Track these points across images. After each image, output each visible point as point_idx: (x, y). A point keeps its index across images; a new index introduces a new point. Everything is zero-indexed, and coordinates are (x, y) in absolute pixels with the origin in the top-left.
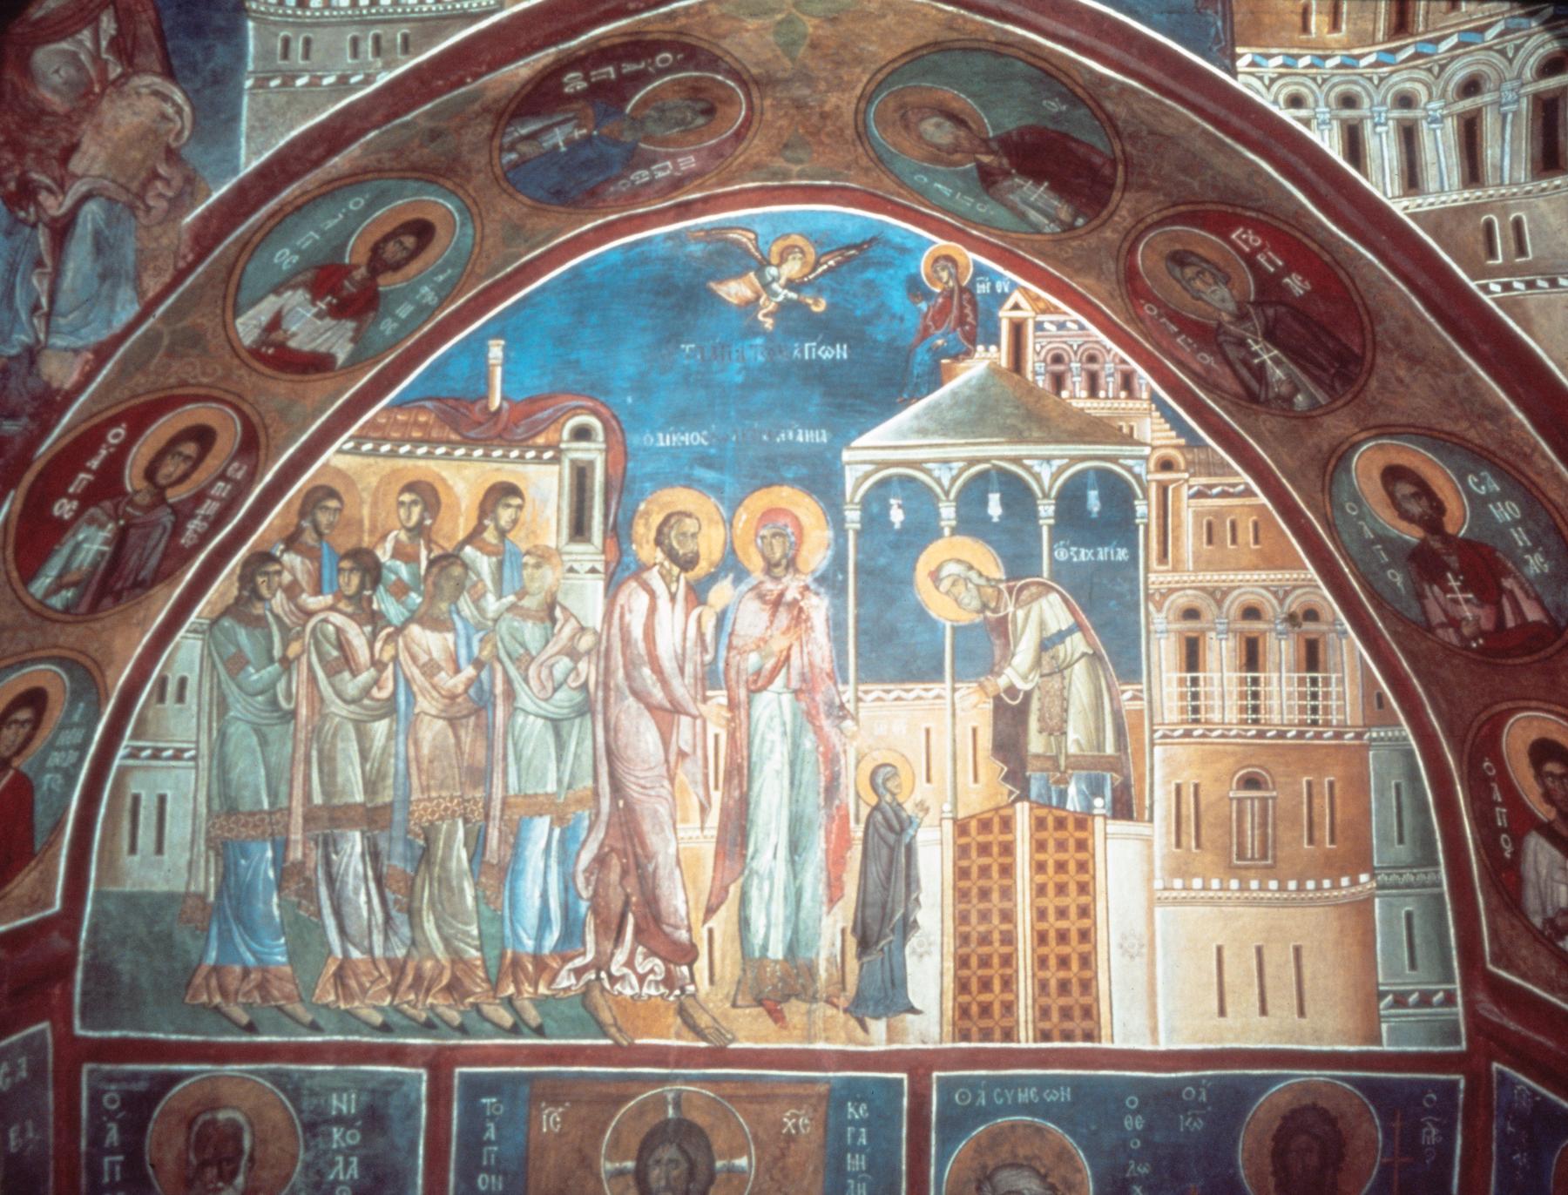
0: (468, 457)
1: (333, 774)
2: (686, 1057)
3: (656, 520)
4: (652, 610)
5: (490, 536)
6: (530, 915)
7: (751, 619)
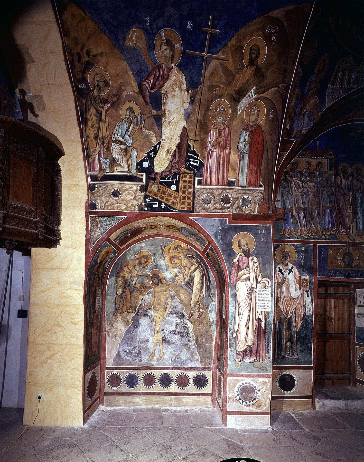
0: (314, 158)
1: (298, 203)
2: (349, 243)
3: (341, 167)
4: (341, 180)
5: (318, 169)
6: (327, 223)
7: (355, 182)
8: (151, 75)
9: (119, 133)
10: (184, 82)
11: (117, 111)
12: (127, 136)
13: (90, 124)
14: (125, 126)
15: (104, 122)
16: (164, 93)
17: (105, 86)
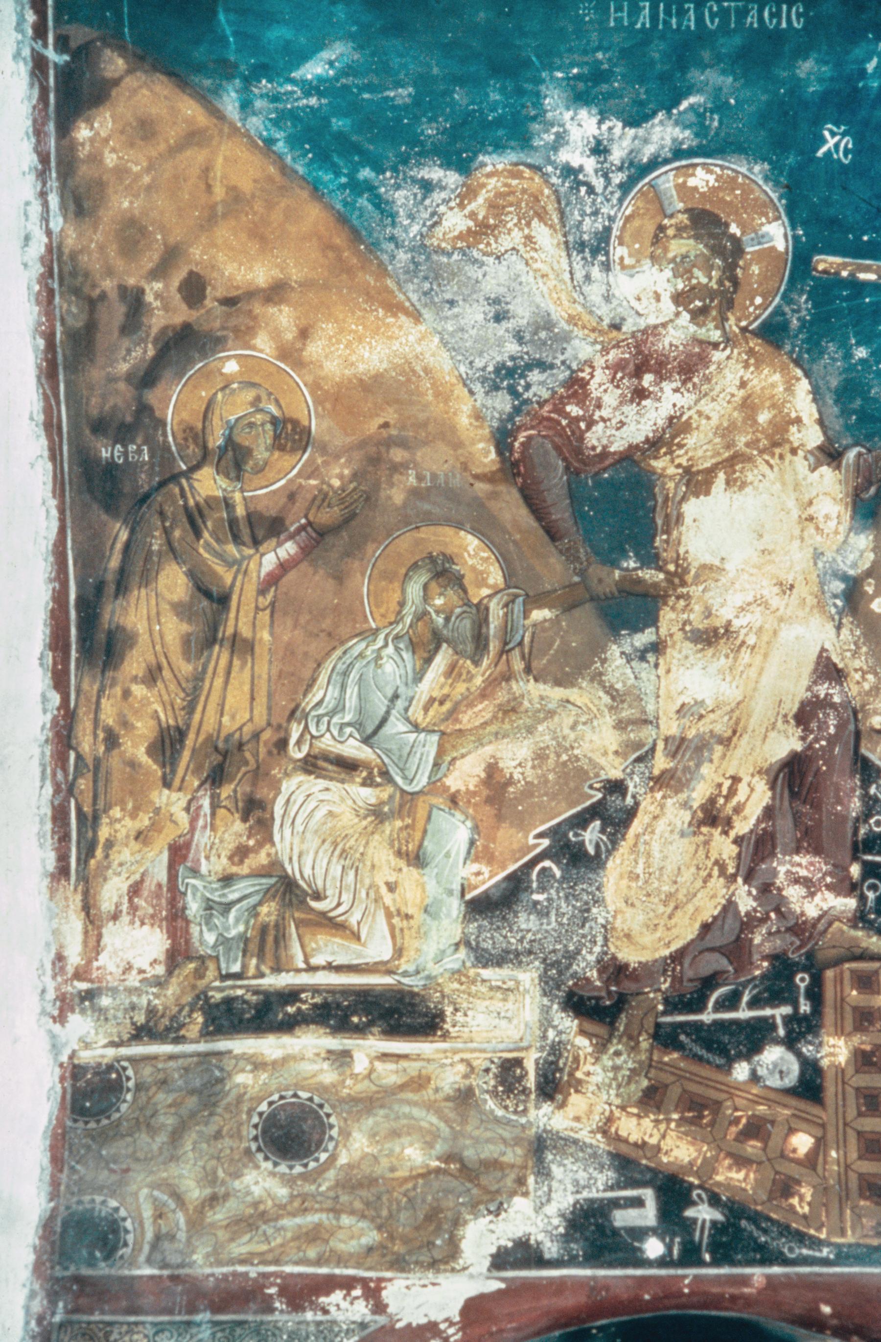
9: (339, 708)
11: (339, 578)
12: (402, 727)
13: (134, 664)
14: (389, 667)
15: (241, 646)
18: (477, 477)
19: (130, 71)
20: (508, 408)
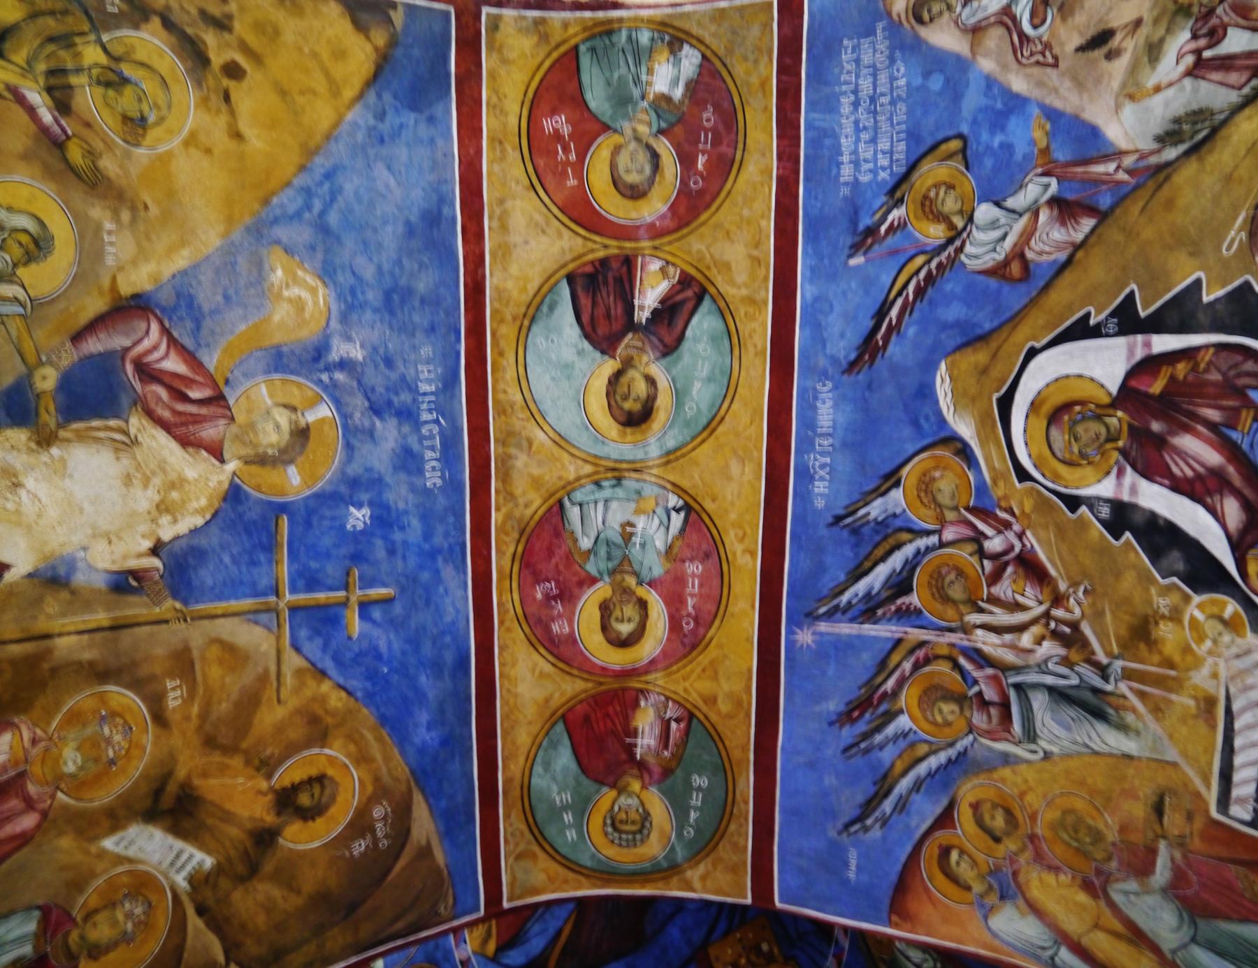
8: (186, 361)
10: (183, 527)
11: (26, 157)
16: (133, 431)
17: (126, 119)
18: (114, 279)
19: (376, 49)
20: (164, 303)
